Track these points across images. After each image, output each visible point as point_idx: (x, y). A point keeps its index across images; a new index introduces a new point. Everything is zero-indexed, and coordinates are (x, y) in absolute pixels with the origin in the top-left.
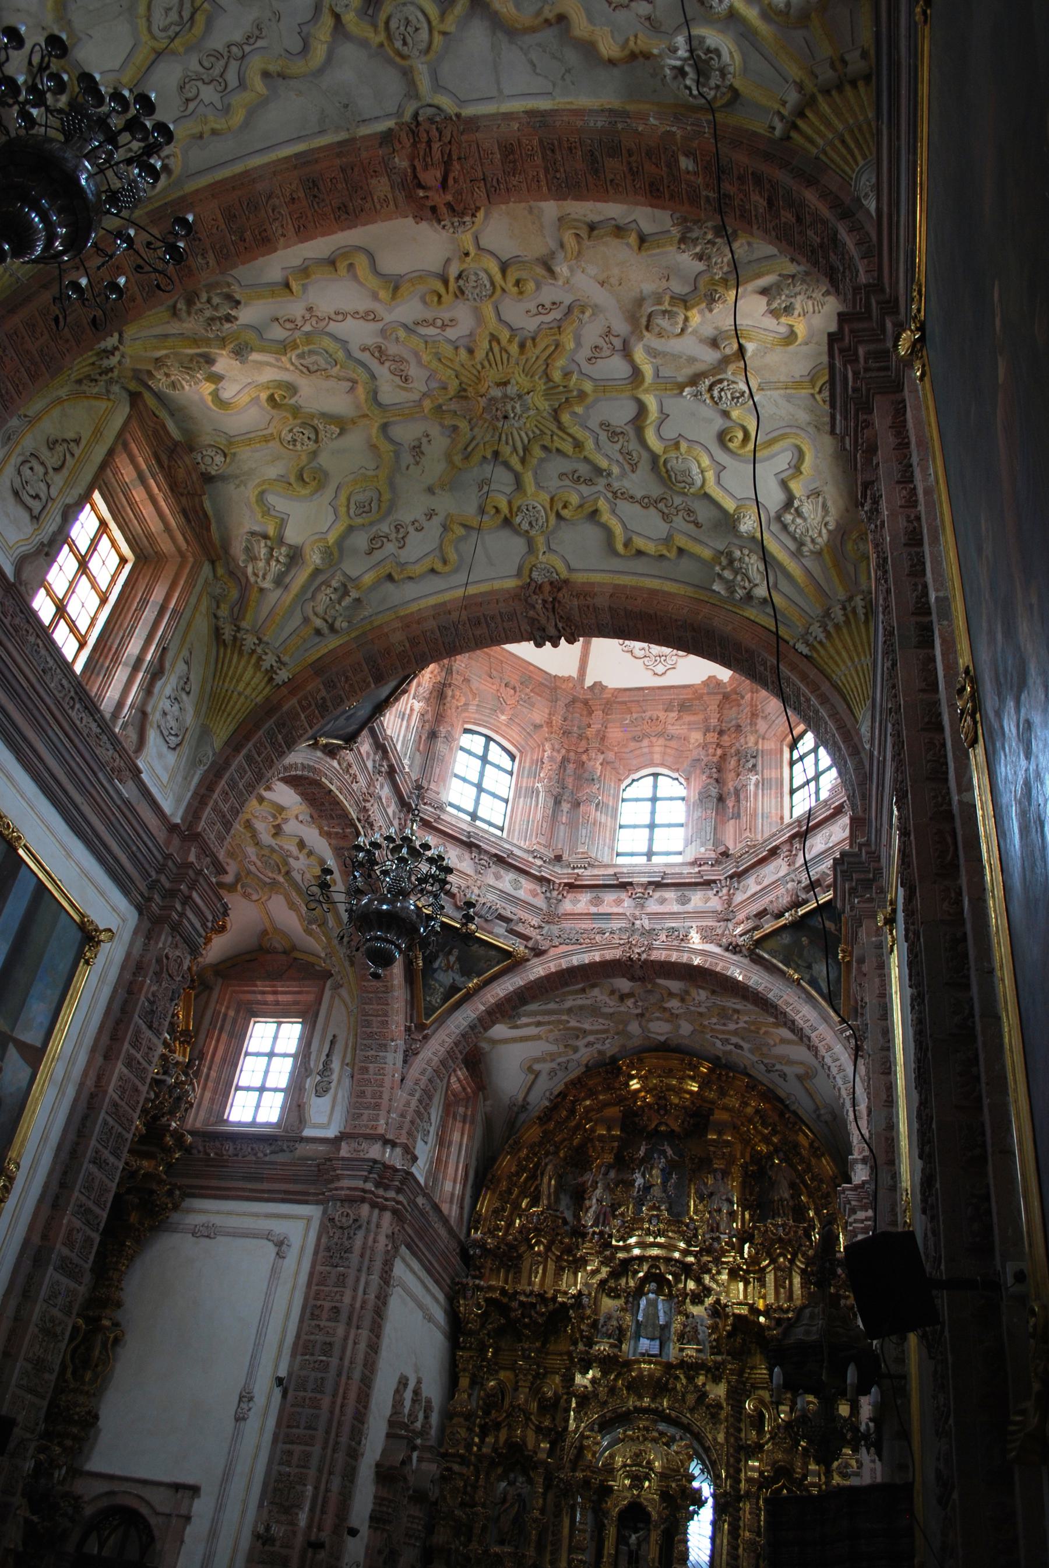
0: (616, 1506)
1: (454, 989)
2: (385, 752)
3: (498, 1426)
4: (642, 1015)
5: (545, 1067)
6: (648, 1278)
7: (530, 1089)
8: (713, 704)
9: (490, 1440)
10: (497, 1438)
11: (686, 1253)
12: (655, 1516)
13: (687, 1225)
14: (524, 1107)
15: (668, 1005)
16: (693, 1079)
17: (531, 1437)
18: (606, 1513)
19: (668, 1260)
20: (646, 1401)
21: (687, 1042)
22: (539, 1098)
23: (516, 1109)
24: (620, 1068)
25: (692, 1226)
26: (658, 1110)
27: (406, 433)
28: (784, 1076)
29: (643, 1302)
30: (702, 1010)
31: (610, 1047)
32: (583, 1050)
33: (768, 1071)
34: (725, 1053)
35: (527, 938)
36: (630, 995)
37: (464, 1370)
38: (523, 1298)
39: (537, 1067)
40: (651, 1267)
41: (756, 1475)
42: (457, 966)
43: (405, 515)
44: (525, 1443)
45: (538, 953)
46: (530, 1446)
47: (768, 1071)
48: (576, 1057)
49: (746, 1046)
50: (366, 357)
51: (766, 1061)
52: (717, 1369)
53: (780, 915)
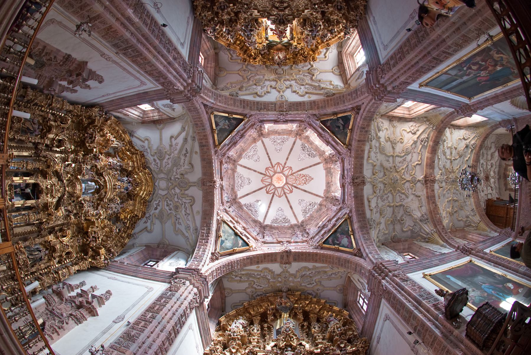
1: (217, 125)
2: (284, 122)
5: (146, 144)
8: (234, 197)
15: (176, 188)
21: (156, 192)
22: (134, 140)
27: (391, 159)
28: (146, 222)
31: (152, 166)
32: (152, 158)
33: (146, 218)
35: (220, 150)
39: (146, 142)
42: (223, 127)
43: (379, 155)
45: (216, 152)
47: (146, 218)
48: (149, 155)
49: (157, 211)
50: (404, 157)
53: (236, 229)
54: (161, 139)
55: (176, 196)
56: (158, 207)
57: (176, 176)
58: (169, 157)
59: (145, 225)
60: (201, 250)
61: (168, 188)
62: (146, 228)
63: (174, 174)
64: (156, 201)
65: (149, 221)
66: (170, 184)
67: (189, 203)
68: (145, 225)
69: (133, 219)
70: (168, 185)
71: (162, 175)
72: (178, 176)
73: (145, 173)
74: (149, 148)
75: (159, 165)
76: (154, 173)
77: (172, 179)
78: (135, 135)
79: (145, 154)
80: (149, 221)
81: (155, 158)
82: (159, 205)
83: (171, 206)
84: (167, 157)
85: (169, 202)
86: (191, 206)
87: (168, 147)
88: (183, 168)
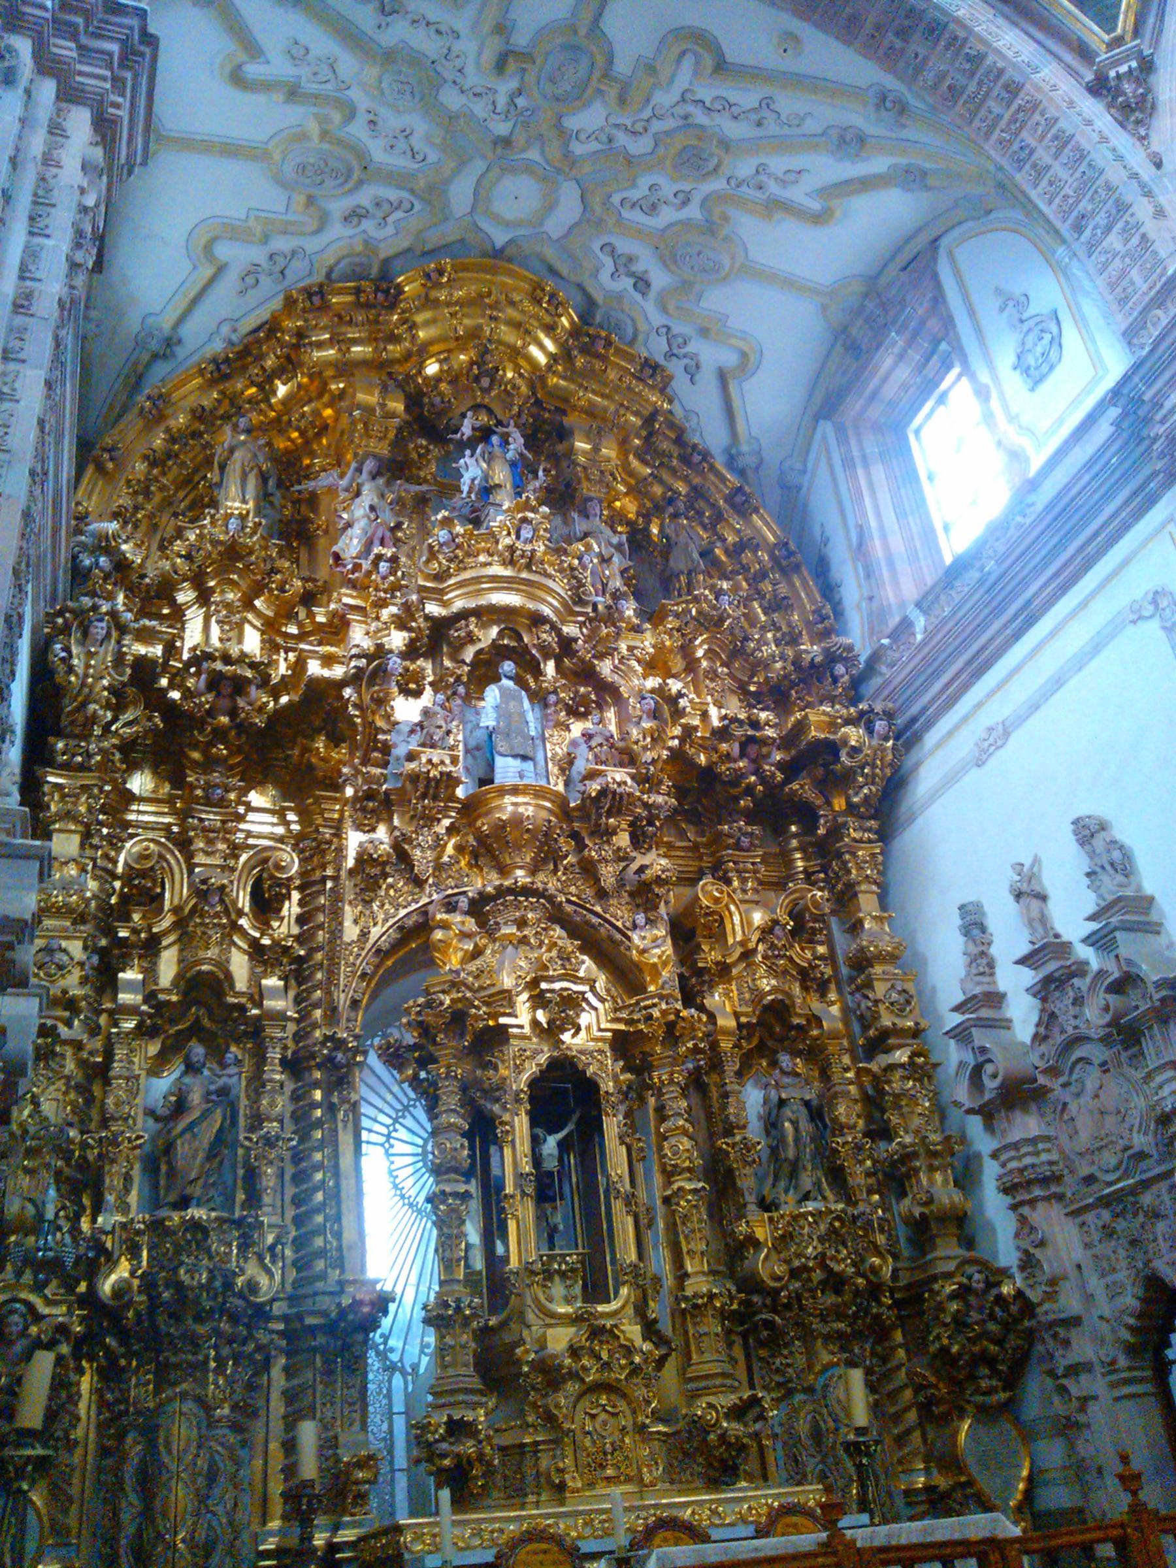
0: (519, 1069)
3: (152, 947)
4: (506, 142)
6: (498, 652)
7: (195, 301)
9: (130, 975)
10: (151, 972)
11: (568, 612)
12: (608, 1086)
13: (580, 558)
14: (171, 343)
15: (572, 123)
16: (550, 329)
17: (240, 965)
18: (496, 1092)
19: (537, 620)
20: (521, 876)
21: (550, 254)
23: (154, 345)
24: (399, 289)
25: (586, 559)
26: (477, 379)
29: (492, 694)
30: (640, 146)
33: (670, 355)
34: (608, 293)
36: (525, 56)
37: (68, 815)
38: (219, 666)
39: (224, 251)
40: (501, 634)
41: (732, 1023)
44: (229, 976)
46: (241, 984)
47: (670, 355)
49: (660, 279)
51: (676, 329)
52: (651, 823)
54: (230, 150)
55: (622, 139)
56: (638, 268)
57: (502, 101)
58: (362, 118)
59: (707, 377)
60: (1043, 155)
61: (549, 178)
62: (723, 377)
63: (480, 109)
64: (595, 274)
65: (690, 348)
66: (533, 154)
67: (696, 73)
68: (707, 377)
69: (665, 445)
70: (529, 168)
71: (461, 194)
72: (505, 87)
73: (428, 302)
74: (265, 239)
75: (393, 194)
76: (434, 238)
77: (502, 128)
78: (166, 323)
79: (300, 275)
80: (690, 348)
81: (338, 207)
82: (631, 259)
83: (668, 189)
84: (358, 130)
85: (635, 194)
86: (721, 67)
87: (297, 115)
88: (467, 46)
